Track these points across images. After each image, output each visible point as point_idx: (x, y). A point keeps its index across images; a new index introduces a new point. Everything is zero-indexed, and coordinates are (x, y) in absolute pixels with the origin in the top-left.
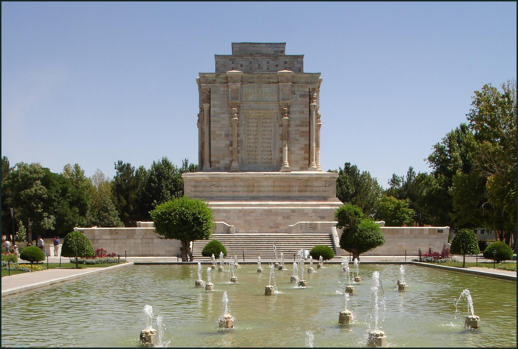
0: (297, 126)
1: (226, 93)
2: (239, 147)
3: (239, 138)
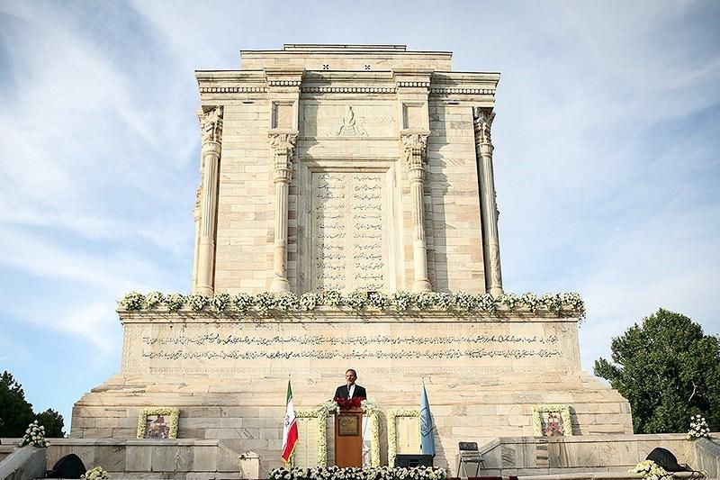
2: (295, 245)
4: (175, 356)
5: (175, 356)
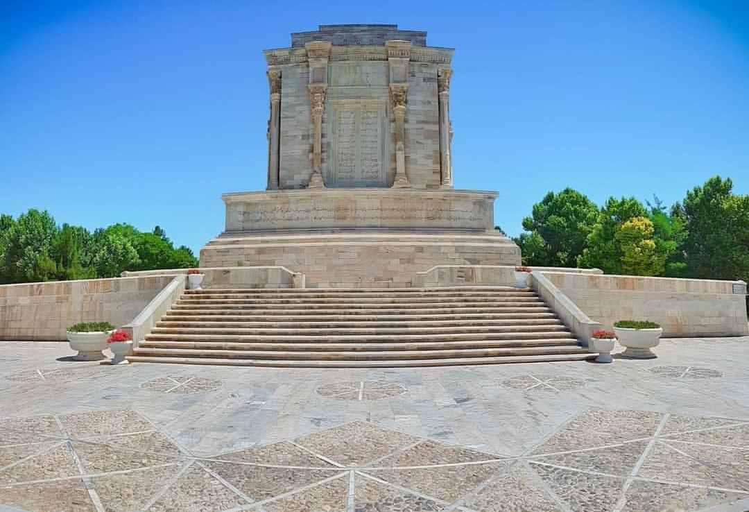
0: (419, 122)
1: (306, 75)
3: (325, 140)
4: (258, 221)
5: (258, 221)
